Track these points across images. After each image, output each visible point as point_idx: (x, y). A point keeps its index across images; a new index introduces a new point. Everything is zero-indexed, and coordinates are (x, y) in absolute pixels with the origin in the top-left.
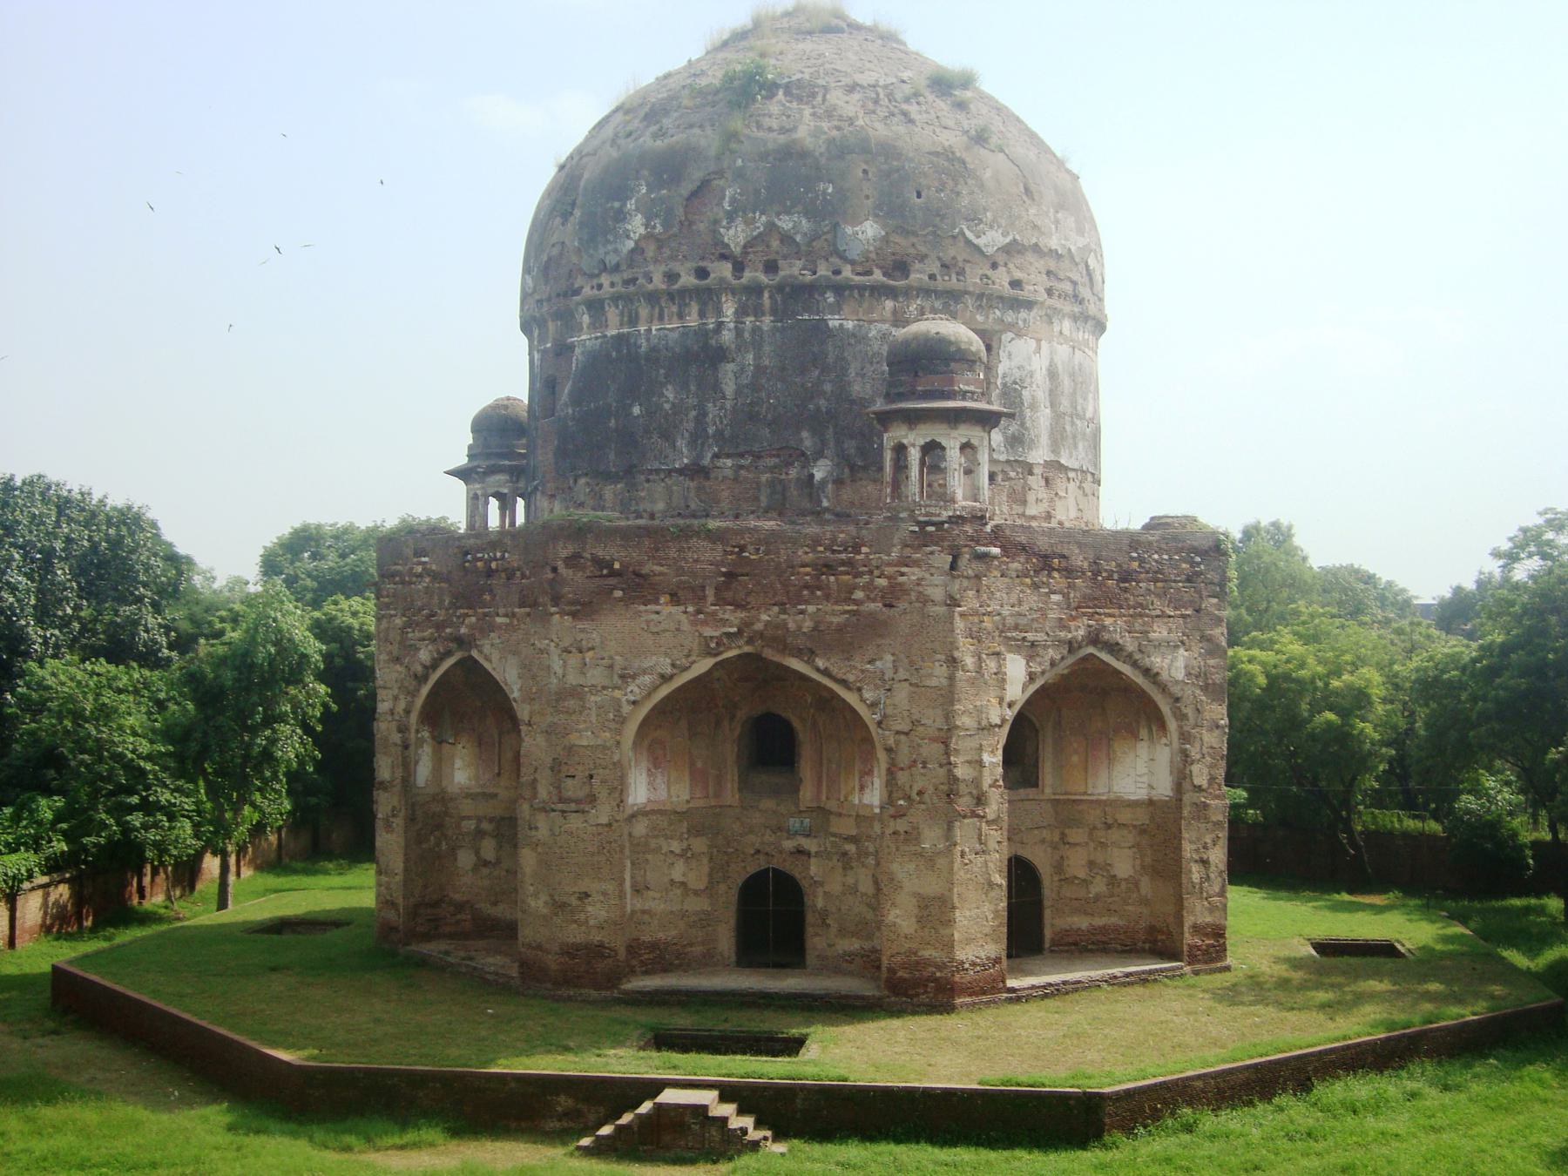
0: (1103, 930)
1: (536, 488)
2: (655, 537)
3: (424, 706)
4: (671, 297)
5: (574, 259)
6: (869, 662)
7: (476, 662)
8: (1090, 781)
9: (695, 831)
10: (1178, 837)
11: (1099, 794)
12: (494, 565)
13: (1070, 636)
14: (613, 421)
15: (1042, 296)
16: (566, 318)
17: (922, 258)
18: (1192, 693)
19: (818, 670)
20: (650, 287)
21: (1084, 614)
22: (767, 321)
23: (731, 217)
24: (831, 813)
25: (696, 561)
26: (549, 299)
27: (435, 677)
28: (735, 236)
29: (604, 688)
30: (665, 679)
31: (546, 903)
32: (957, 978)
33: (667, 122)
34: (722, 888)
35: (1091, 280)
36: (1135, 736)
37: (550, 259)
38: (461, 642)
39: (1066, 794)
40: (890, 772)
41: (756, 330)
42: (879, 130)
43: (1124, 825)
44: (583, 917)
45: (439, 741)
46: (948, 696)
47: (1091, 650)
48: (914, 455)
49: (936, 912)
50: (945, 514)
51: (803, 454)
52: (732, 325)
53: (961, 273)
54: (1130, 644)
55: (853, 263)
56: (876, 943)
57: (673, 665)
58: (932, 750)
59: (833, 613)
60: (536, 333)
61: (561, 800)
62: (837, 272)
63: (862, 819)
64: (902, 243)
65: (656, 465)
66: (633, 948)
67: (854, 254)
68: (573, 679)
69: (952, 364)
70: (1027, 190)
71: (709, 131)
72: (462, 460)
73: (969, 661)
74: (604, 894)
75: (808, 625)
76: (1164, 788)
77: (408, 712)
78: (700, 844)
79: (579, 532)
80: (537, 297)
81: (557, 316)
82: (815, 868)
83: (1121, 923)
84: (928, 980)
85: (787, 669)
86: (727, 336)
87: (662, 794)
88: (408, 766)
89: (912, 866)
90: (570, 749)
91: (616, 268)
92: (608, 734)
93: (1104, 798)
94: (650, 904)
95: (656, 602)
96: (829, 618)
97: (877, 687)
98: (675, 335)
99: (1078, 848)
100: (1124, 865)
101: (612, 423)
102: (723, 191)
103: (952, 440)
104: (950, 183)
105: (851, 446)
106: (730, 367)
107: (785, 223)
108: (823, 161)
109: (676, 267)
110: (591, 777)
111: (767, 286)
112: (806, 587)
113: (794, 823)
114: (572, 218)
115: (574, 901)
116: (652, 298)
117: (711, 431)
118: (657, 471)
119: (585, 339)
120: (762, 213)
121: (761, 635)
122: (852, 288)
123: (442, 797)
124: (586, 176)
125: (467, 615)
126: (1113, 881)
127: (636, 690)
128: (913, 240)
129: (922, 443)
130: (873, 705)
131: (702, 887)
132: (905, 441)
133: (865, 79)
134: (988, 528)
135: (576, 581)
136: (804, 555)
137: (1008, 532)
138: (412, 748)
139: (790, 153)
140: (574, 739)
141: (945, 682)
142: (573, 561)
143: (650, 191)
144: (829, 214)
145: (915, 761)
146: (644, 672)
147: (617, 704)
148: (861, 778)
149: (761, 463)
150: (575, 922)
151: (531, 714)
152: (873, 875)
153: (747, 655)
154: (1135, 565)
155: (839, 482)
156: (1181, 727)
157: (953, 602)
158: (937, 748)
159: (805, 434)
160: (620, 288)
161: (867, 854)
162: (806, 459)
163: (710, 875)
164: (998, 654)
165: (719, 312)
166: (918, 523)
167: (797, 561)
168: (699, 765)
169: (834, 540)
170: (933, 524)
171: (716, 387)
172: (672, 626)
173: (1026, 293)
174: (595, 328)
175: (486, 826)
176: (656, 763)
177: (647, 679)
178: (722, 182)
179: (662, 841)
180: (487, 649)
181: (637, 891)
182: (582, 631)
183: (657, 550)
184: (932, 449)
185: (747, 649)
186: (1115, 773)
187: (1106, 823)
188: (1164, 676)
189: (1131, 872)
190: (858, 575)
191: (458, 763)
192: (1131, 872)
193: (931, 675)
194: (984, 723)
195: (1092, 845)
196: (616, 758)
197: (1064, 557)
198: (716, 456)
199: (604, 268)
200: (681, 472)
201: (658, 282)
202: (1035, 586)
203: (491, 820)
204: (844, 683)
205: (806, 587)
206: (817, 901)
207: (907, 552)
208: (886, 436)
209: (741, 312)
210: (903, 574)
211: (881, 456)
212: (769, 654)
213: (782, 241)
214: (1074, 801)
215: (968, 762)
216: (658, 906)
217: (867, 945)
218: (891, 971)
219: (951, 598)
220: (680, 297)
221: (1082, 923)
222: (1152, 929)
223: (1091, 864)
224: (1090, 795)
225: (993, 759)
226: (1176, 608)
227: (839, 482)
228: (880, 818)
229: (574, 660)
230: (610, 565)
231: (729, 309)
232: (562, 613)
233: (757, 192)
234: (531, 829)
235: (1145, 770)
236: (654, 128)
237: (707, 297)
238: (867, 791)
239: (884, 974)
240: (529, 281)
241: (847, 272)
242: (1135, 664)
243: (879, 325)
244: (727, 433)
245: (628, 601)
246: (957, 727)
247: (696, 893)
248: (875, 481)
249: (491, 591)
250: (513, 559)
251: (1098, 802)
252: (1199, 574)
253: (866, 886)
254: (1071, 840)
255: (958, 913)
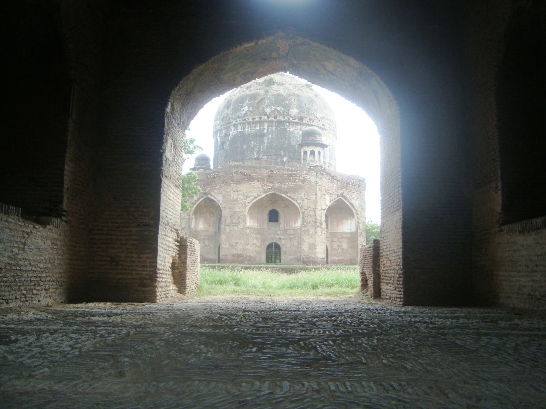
0: (341, 260)
1: (218, 166)
2: (254, 168)
3: (195, 210)
4: (253, 123)
5: (231, 116)
6: (299, 195)
7: (209, 197)
9: (258, 233)
10: (357, 239)
12: (216, 176)
14: (239, 149)
15: (328, 129)
16: (228, 129)
17: (306, 117)
18: (359, 209)
19: (288, 196)
20: (249, 121)
21: (340, 190)
22: (274, 129)
23: (267, 107)
24: (287, 230)
25: (263, 173)
26: (223, 125)
27: (197, 203)
28: (268, 111)
29: (242, 199)
30: (255, 198)
31: (228, 245)
32: (317, 261)
33: (251, 89)
34: (263, 246)
35: (336, 127)
36: (348, 219)
37: (224, 117)
38: (205, 194)
40: (303, 217)
41: (271, 130)
42: (297, 92)
44: (237, 248)
45: (196, 219)
46: (315, 202)
47: (341, 197)
48: (308, 153)
49: (313, 247)
50: (315, 165)
51: (281, 156)
52: (266, 129)
53: (313, 121)
54: (348, 197)
55: (292, 117)
56: (299, 255)
57: (257, 195)
58: (312, 213)
59: (291, 184)
60: (219, 133)
61: (232, 223)
62: (289, 119)
63: (295, 230)
64: (302, 114)
65: (249, 158)
66: (247, 256)
67: (292, 115)
68: (236, 197)
69: (316, 135)
70: (325, 107)
71: (261, 90)
72: (193, 167)
73: (319, 195)
74: (241, 243)
75: (286, 187)
76: (354, 230)
77: (190, 211)
78: (259, 236)
79: (238, 167)
80: (220, 125)
81: (225, 128)
82: (283, 242)
83: (345, 258)
84: (311, 261)
85: (282, 196)
86: (265, 131)
87: (252, 225)
88: (190, 224)
89: (308, 237)
90: (235, 212)
91: (241, 117)
92: (243, 209)
94: (249, 248)
95: (254, 182)
96: (290, 185)
97: (300, 200)
98: (254, 131)
100: (345, 246)
101: (239, 149)
102: (265, 102)
103: (316, 150)
104: (311, 104)
105: (291, 154)
106: (266, 137)
107: (278, 108)
108: (286, 97)
109: (255, 117)
110: (239, 218)
111: (275, 121)
112: (286, 179)
113: (279, 232)
114: (230, 109)
115: (235, 245)
116: (249, 123)
117: (262, 150)
118: (250, 159)
119: (233, 132)
120: (274, 106)
121: (276, 189)
122: (292, 122)
123: (197, 231)
124: (233, 99)
125: (208, 188)
126: (343, 249)
127: (249, 200)
128: (304, 114)
129: (310, 150)
130: (299, 204)
131: (259, 245)
132: (306, 150)
133: (293, 83)
134: (323, 169)
135: (237, 177)
136: (285, 172)
137: (326, 170)
138: (191, 220)
139: (279, 95)
140: (236, 210)
141: (315, 199)
142: (236, 173)
143: (249, 102)
144: (288, 107)
145: (308, 216)
146: (251, 196)
147: (245, 203)
148: (295, 221)
149: (272, 157)
150: (235, 249)
151: (225, 206)
152: (298, 241)
153: (273, 193)
154: (349, 181)
155: (289, 162)
156: (357, 216)
157: (316, 183)
158: (313, 212)
159: (282, 152)
160: (242, 121)
161: (296, 237)
162: (282, 157)
163: (261, 243)
164: (324, 195)
165: (264, 126)
166: (309, 166)
167: (284, 174)
168: (259, 219)
169: (292, 170)
170: (313, 167)
171: (263, 141)
172: (257, 187)
173: (325, 127)
174: (235, 130)
175: (206, 237)
176: (251, 218)
177: (252, 198)
178: (265, 100)
179: (251, 234)
180: (213, 194)
181: (247, 244)
182: (238, 187)
183: (254, 171)
184: (312, 153)
185: (273, 192)
188: (354, 205)
189: (346, 247)
190: (297, 177)
191: (200, 224)
192: (346, 247)
193: (312, 197)
194: (322, 208)
195: (338, 242)
196: (245, 214)
197: (336, 177)
198: (263, 156)
199: (238, 117)
200: (255, 159)
201: (251, 120)
202: (331, 182)
203: (207, 236)
204: (293, 199)
205: (286, 179)
206: (283, 249)
207: (307, 172)
208: (302, 149)
209: (268, 127)
210: (306, 177)
211: (300, 154)
212: (278, 193)
213: (278, 112)
215: (319, 216)
216: (251, 248)
217: (296, 256)
218: (303, 259)
219: (316, 182)
220: (255, 123)
221: (336, 258)
222: (351, 259)
223: (338, 246)
225: (324, 216)
226: (356, 191)
227: (289, 162)
228: (300, 229)
229: (236, 193)
230: (244, 174)
231: (266, 126)
232: (233, 183)
233: (272, 102)
234: (224, 230)
236: (249, 90)
237: (261, 123)
238: (296, 224)
239: (302, 260)
240: (218, 122)
241: (291, 119)
242: (349, 202)
243: (297, 130)
244: (265, 151)
245: (248, 181)
246: (317, 208)
247: (258, 247)
248: (296, 162)
249: (215, 181)
250: (220, 174)
251: (340, 233)
252: (360, 185)
253: (296, 243)
255: (317, 247)
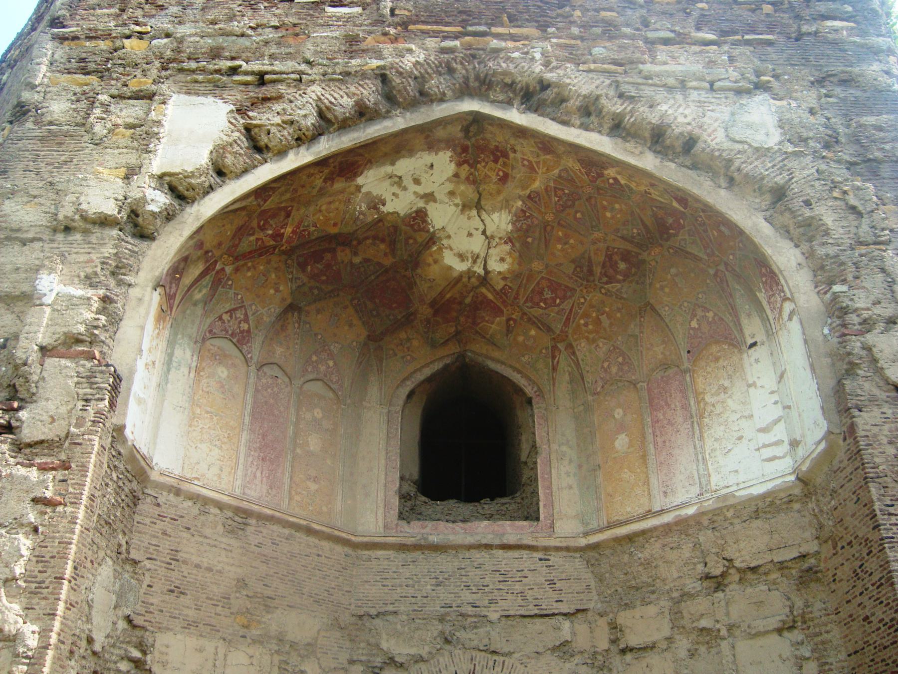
8: (654, 481)
11: (678, 507)
13: (375, 63)
39: (610, 527)
43: (754, 570)
93: (691, 511)
99: (653, 659)
186: (709, 444)
187: (708, 577)
214: (630, 538)
224: (662, 512)
235: (778, 411)
251: (683, 526)
254: (633, 640)
